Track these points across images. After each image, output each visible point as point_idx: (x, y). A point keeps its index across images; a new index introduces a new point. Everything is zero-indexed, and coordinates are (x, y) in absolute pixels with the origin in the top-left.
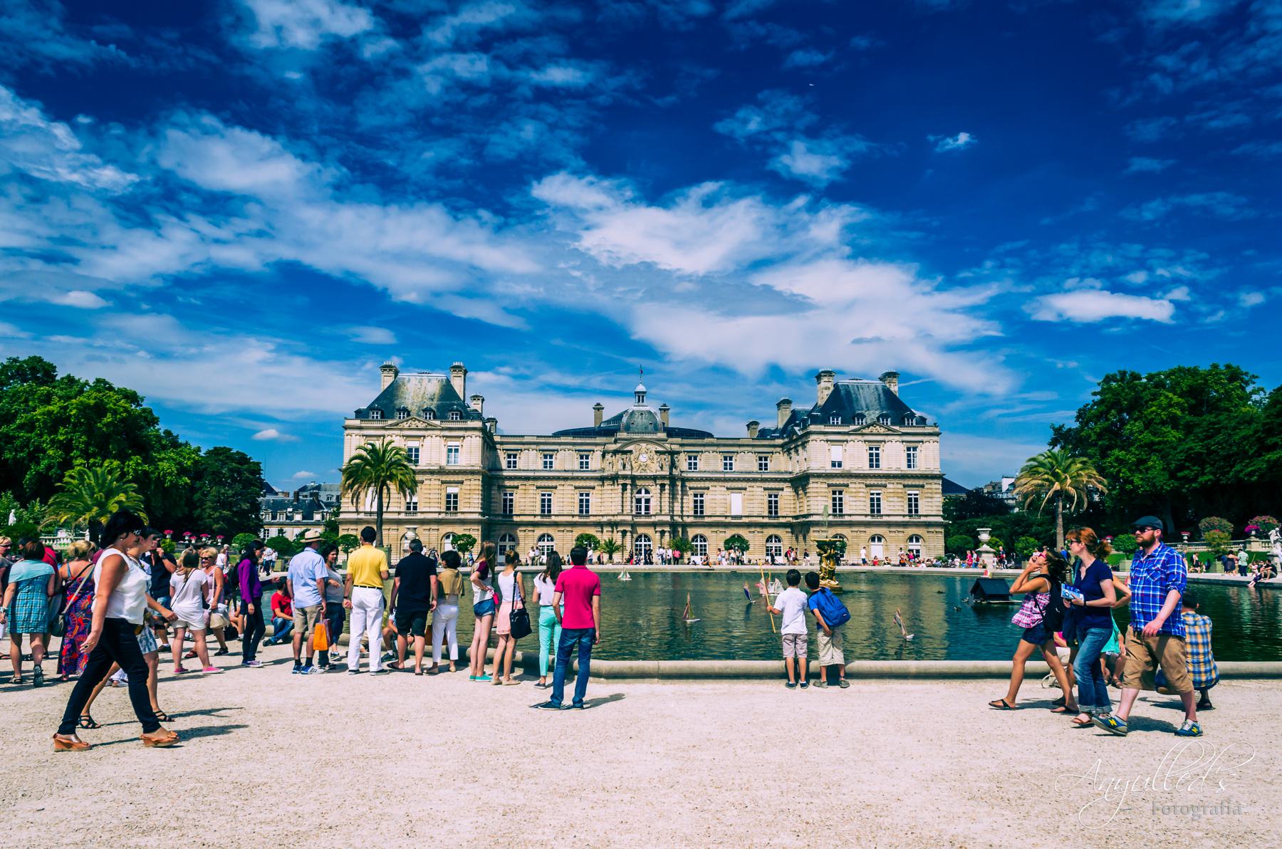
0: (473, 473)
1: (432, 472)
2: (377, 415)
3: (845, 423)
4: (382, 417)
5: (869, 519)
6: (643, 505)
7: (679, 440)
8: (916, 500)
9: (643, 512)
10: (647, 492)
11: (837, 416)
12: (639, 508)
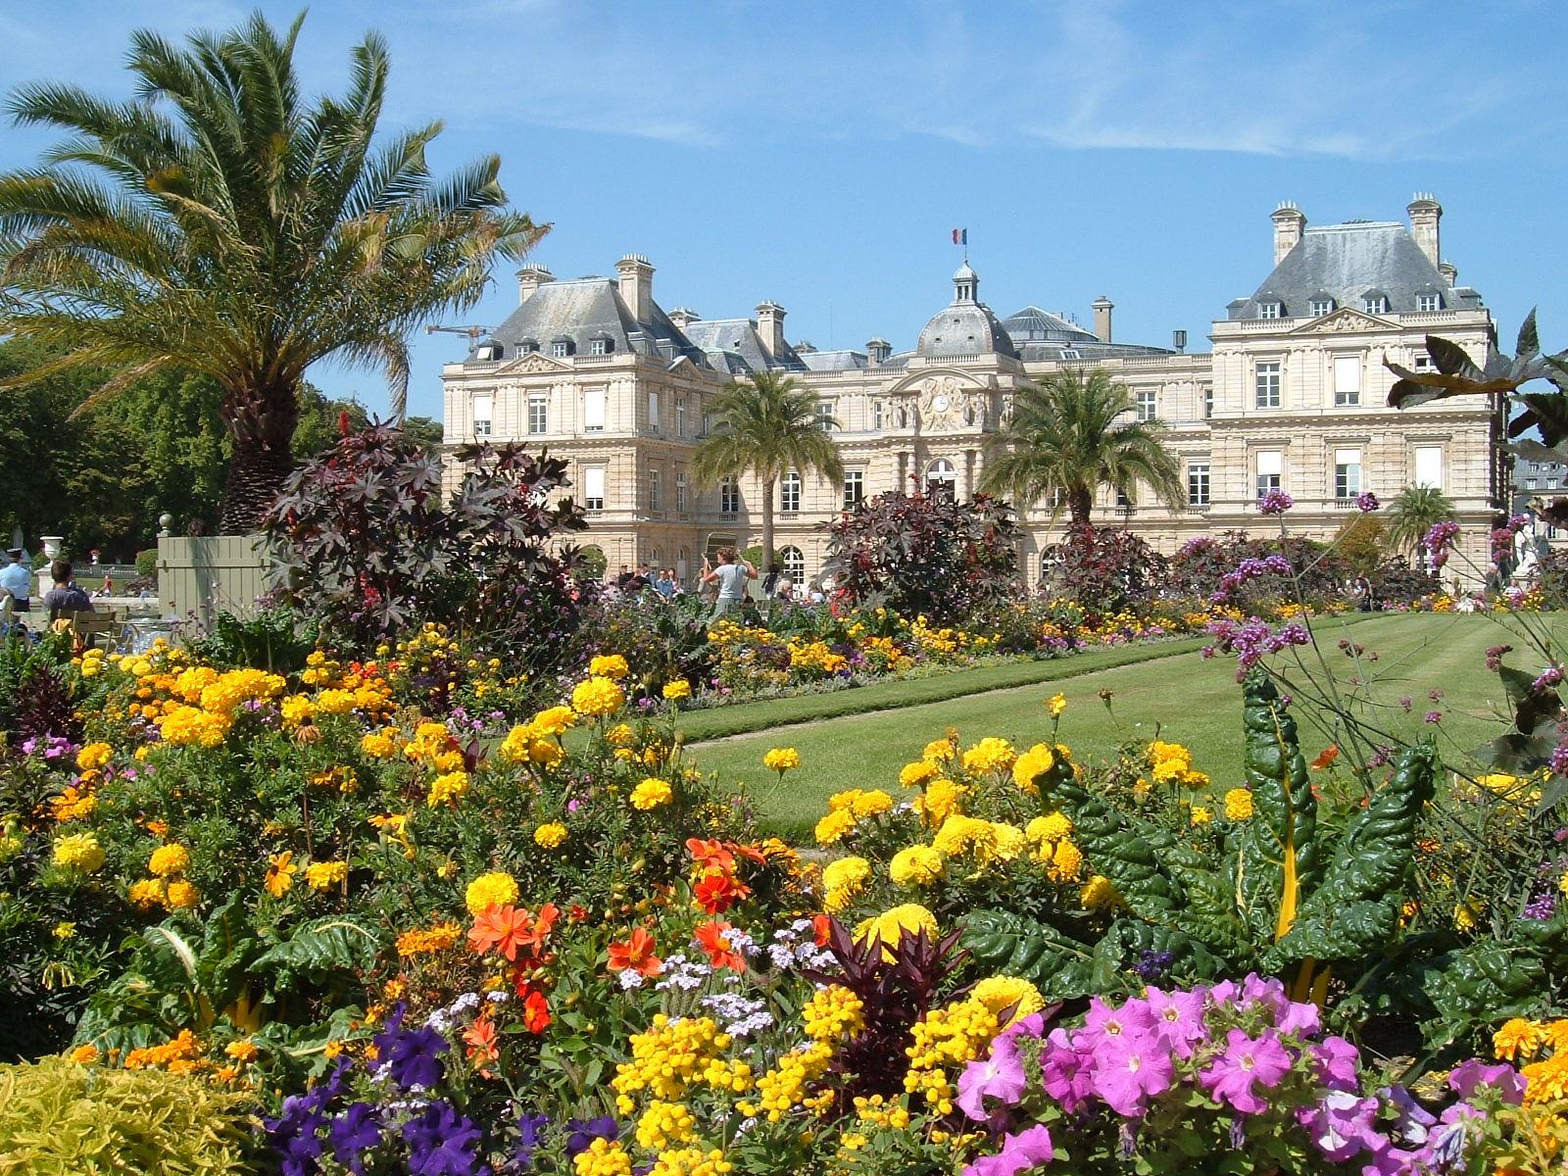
4: (498, 353)
10: (949, 467)
11: (1273, 300)
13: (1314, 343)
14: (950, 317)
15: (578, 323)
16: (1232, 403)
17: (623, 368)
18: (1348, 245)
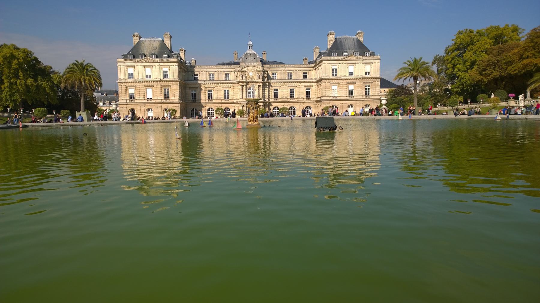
2: (131, 57)
4: (134, 57)
5: (348, 98)
8: (369, 89)
11: (335, 52)
13: (345, 62)
16: (327, 75)
17: (174, 62)
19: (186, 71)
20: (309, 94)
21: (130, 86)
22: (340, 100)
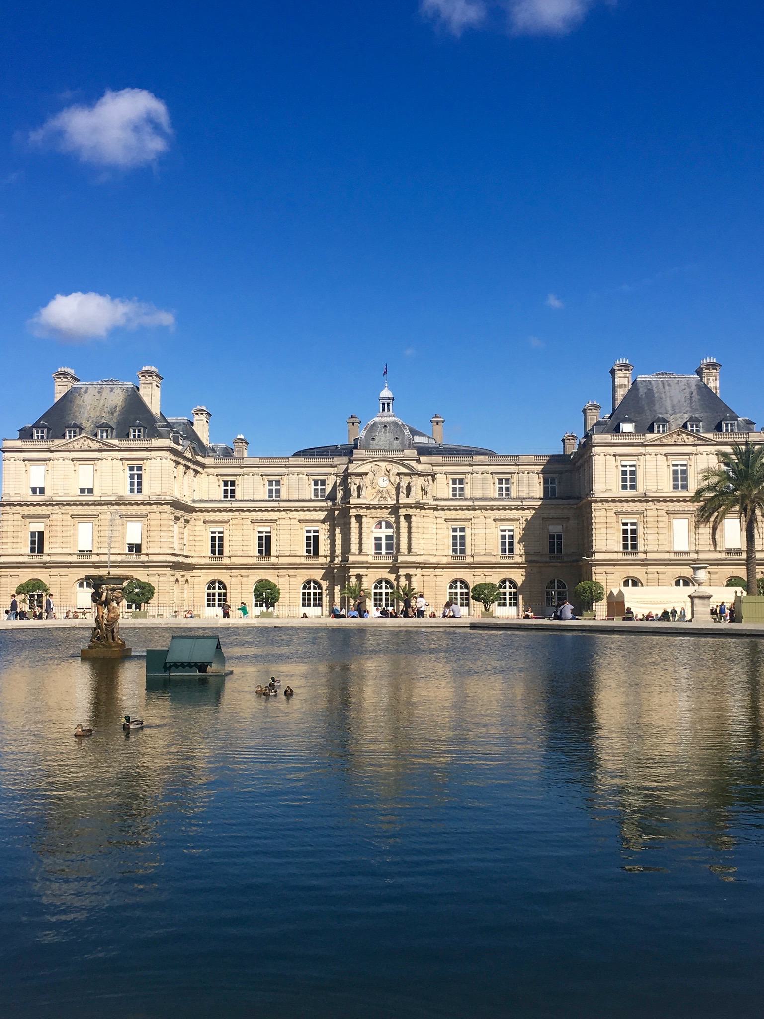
0: (158, 503)
1: (108, 503)
3: (639, 430)
6: (384, 542)
7: (439, 459)
9: (384, 551)
10: (389, 525)
12: (378, 546)
14: (380, 423)
15: (112, 413)
18: (667, 388)
19: (197, 472)
20: (560, 544)
21: (31, 517)
22: (644, 563)
